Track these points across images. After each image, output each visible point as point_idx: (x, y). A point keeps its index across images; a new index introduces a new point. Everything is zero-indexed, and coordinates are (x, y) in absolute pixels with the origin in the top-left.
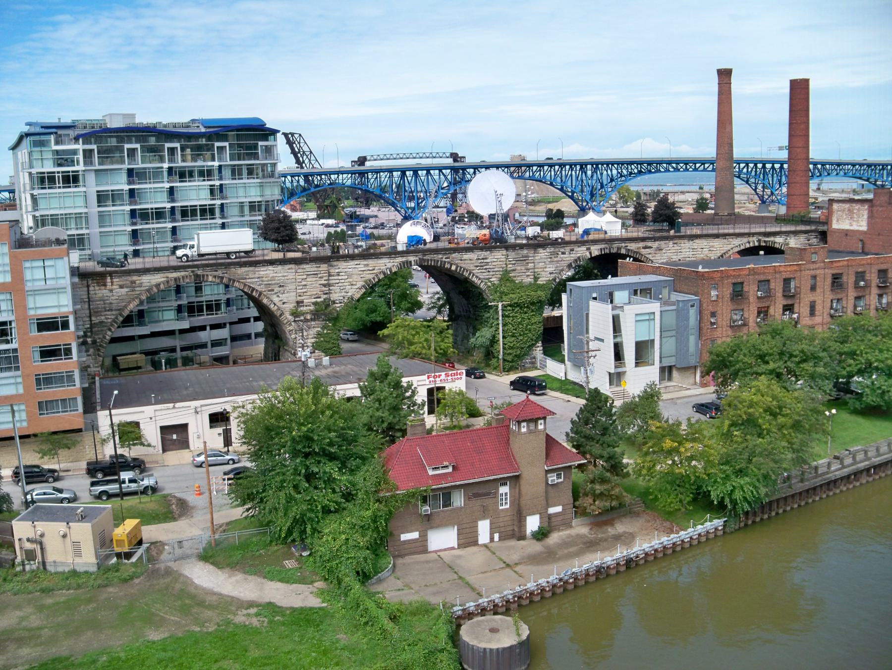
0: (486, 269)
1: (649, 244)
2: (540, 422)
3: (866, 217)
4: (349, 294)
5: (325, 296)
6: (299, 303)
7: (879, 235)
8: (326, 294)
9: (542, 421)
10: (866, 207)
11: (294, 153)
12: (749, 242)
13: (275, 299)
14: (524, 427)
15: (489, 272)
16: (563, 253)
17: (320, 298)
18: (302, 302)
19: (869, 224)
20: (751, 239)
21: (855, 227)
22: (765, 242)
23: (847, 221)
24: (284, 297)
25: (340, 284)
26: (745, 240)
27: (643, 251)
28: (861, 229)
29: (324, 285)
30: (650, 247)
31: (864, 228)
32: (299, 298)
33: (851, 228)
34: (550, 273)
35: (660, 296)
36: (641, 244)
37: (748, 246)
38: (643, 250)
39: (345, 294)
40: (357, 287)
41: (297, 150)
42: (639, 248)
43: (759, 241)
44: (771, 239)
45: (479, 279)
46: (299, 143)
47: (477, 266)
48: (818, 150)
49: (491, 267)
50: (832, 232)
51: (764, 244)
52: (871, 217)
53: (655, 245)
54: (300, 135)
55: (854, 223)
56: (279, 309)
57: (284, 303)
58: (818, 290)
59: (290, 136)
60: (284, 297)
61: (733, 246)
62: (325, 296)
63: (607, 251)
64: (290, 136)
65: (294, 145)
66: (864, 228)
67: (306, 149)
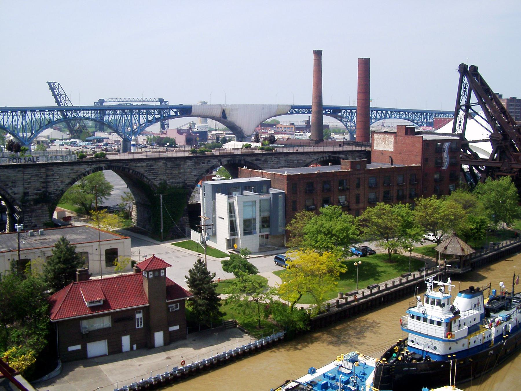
0: (152, 173)
1: (260, 158)
2: (162, 271)
3: (393, 143)
4: (60, 188)
5: (43, 190)
6: (26, 194)
7: (400, 153)
8: (43, 188)
9: (163, 271)
10: (393, 137)
11: (54, 95)
12: (323, 157)
13: (10, 191)
14: (151, 274)
15: (154, 174)
16: (203, 163)
17: (40, 190)
18: (28, 193)
19: (395, 147)
20: (324, 155)
21: (386, 149)
22: (333, 157)
23: (383, 145)
24: (15, 190)
25: (54, 182)
26: (320, 156)
27: (255, 162)
28: (390, 150)
29: (43, 182)
30: (260, 160)
31: (392, 150)
32: (26, 191)
33: (385, 149)
34: (195, 176)
35: (262, 191)
36: (254, 158)
37: (322, 159)
38: (255, 162)
39: (58, 188)
40: (65, 183)
41: (57, 94)
42: (252, 160)
43: (329, 156)
44: (337, 155)
45: (148, 179)
46: (58, 89)
47: (146, 171)
48: (372, 105)
49: (156, 171)
50: (374, 151)
51: (332, 159)
52: (396, 142)
53: (263, 158)
54: (59, 84)
55: (386, 146)
56: (12, 198)
57: (15, 194)
58: (361, 188)
59: (52, 84)
60: (15, 190)
61: (313, 159)
62: (43, 190)
63: (232, 162)
64: (52, 84)
65: (55, 90)
66: (392, 150)
67: (62, 93)
